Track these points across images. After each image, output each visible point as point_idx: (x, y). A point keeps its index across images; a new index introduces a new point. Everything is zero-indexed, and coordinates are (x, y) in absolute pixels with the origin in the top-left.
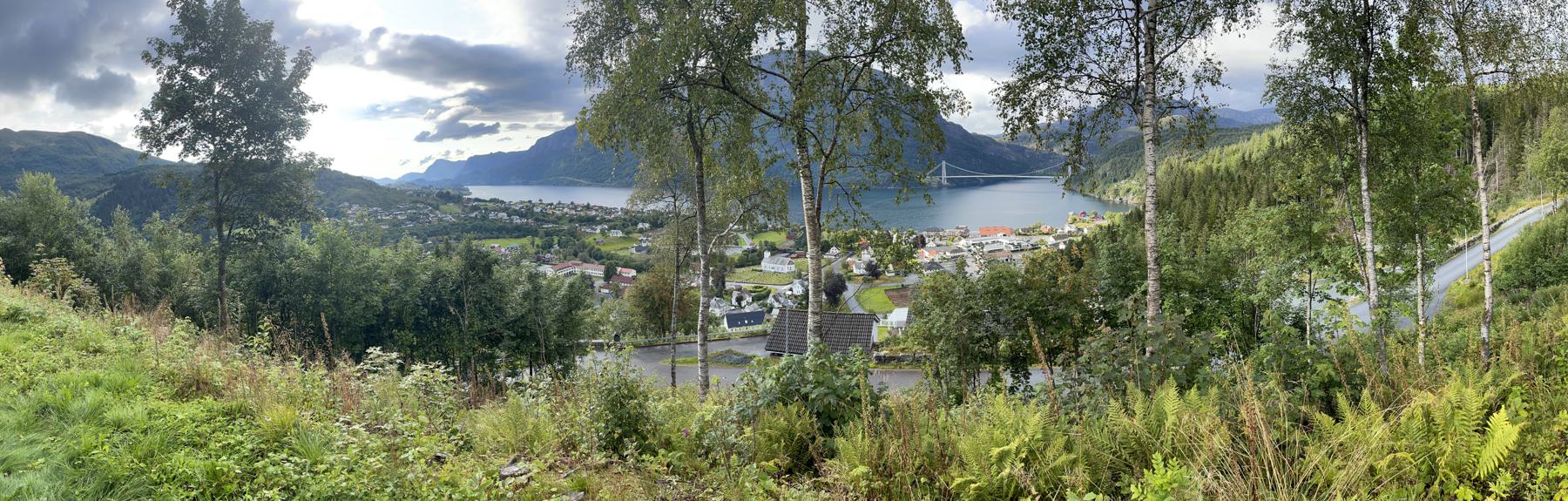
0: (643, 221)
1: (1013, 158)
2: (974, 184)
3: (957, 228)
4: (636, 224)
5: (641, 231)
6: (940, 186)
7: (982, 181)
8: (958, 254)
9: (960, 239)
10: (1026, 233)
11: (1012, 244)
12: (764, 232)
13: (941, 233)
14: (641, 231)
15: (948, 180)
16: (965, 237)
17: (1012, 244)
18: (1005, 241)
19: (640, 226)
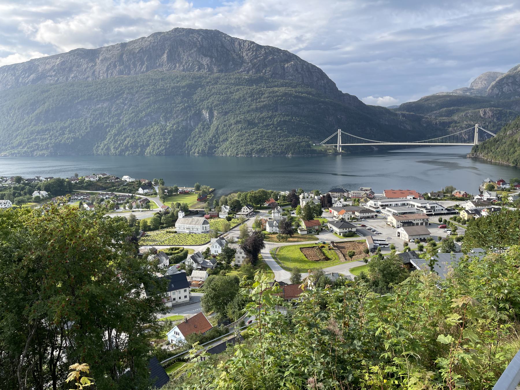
0: (39, 189)
1: (408, 127)
2: (368, 152)
3: (362, 190)
4: (31, 193)
5: (38, 200)
6: (336, 153)
7: (376, 149)
8: (367, 215)
9: (366, 201)
10: (436, 197)
11: (425, 207)
12: (175, 195)
13: (346, 194)
14: (38, 200)
15: (343, 147)
16: (371, 199)
17: (425, 207)
18: (417, 204)
19: (36, 194)
